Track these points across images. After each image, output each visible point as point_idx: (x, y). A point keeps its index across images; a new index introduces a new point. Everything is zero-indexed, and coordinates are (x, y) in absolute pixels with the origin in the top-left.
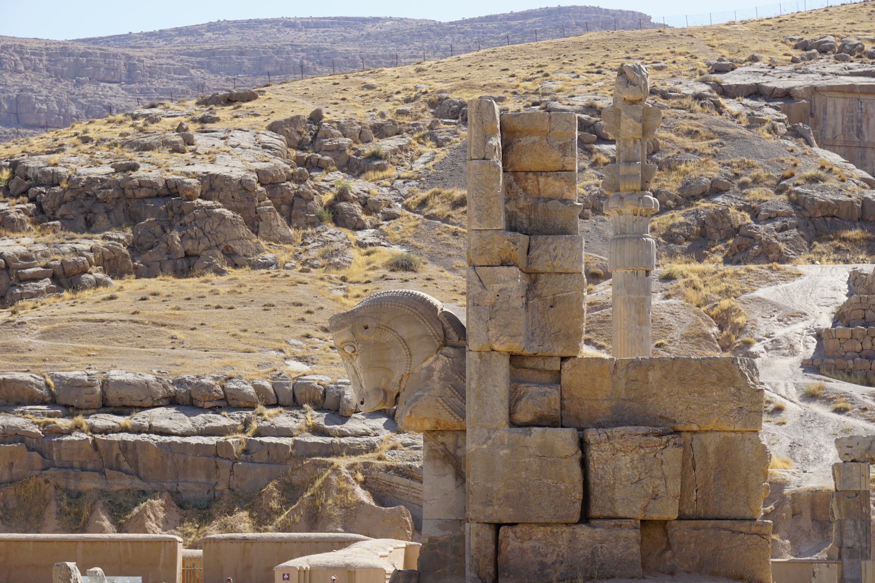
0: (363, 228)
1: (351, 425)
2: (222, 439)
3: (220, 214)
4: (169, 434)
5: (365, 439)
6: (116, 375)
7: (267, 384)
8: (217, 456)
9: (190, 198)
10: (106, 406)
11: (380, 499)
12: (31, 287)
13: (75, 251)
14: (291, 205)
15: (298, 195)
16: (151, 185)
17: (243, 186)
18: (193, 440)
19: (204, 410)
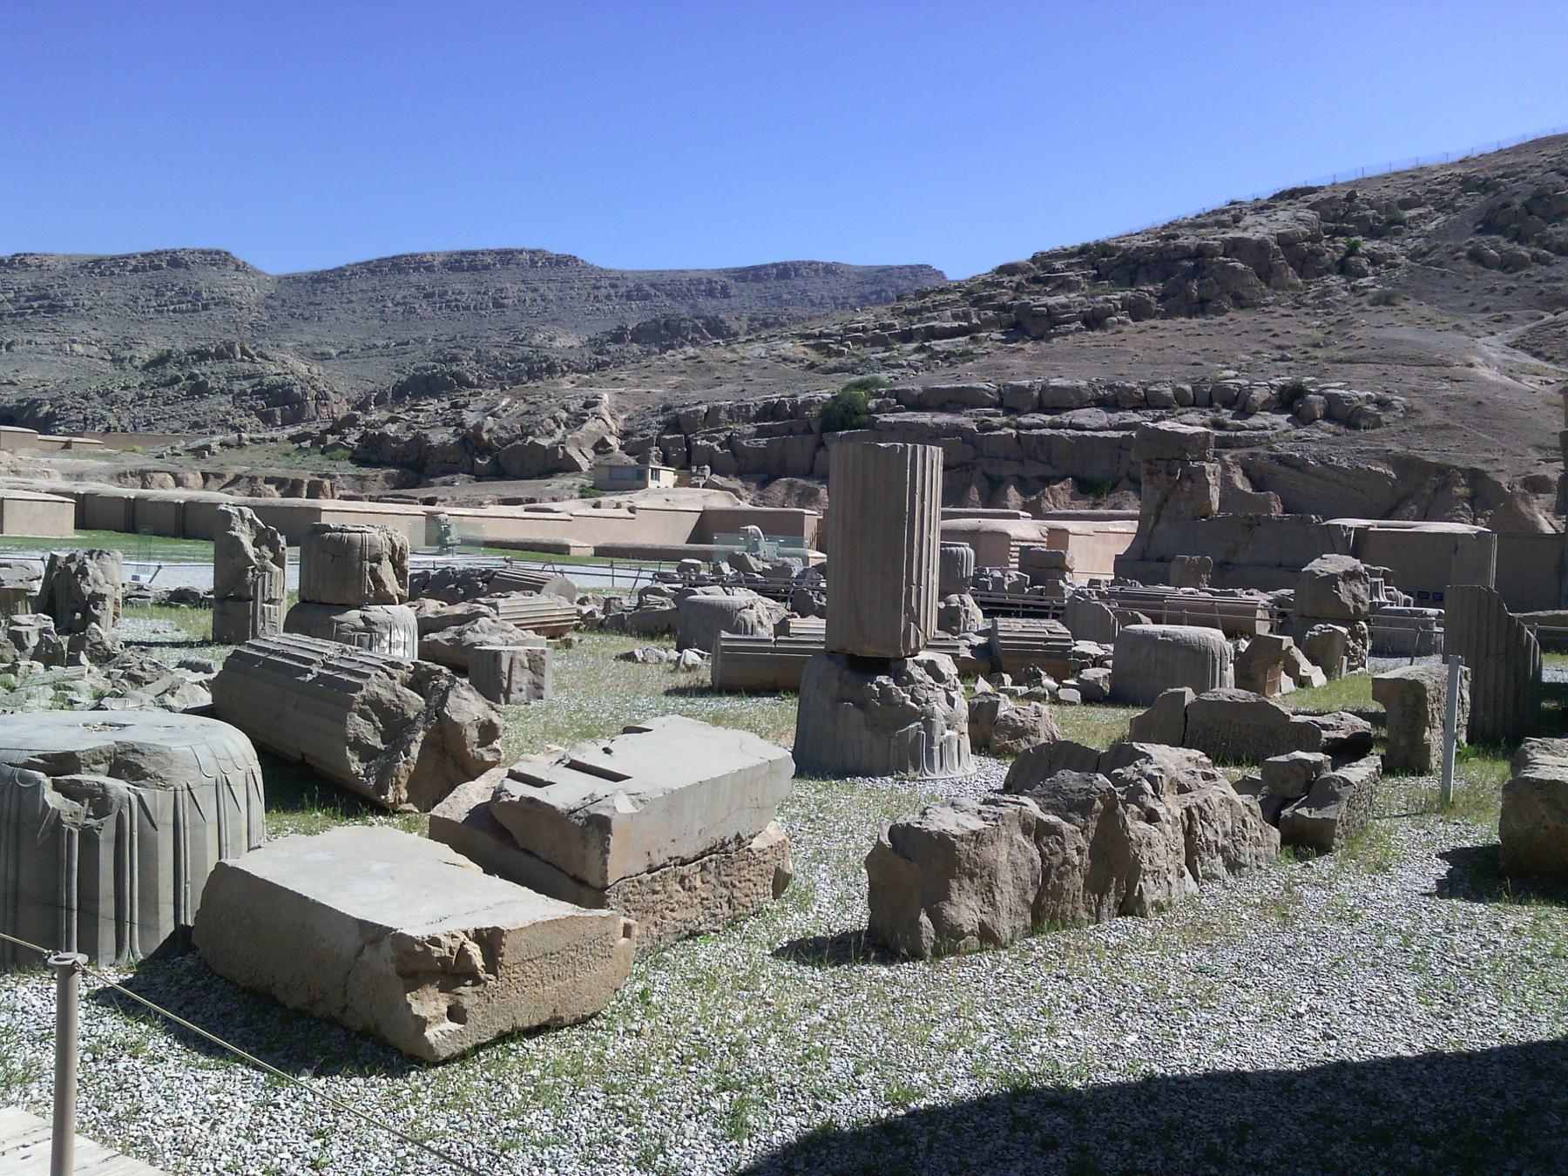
0: (1366, 275)
1: (1254, 421)
2: (1127, 433)
3: (1233, 266)
4: (1084, 429)
5: (1261, 432)
6: (1056, 382)
7: (1188, 387)
8: (1120, 447)
9: (1212, 256)
10: (1041, 408)
11: (1257, 486)
12: (1063, 328)
13: (1108, 300)
14: (1304, 261)
15: (1311, 252)
16: (1184, 248)
17: (1261, 246)
18: (1101, 434)
19: (1124, 409)
